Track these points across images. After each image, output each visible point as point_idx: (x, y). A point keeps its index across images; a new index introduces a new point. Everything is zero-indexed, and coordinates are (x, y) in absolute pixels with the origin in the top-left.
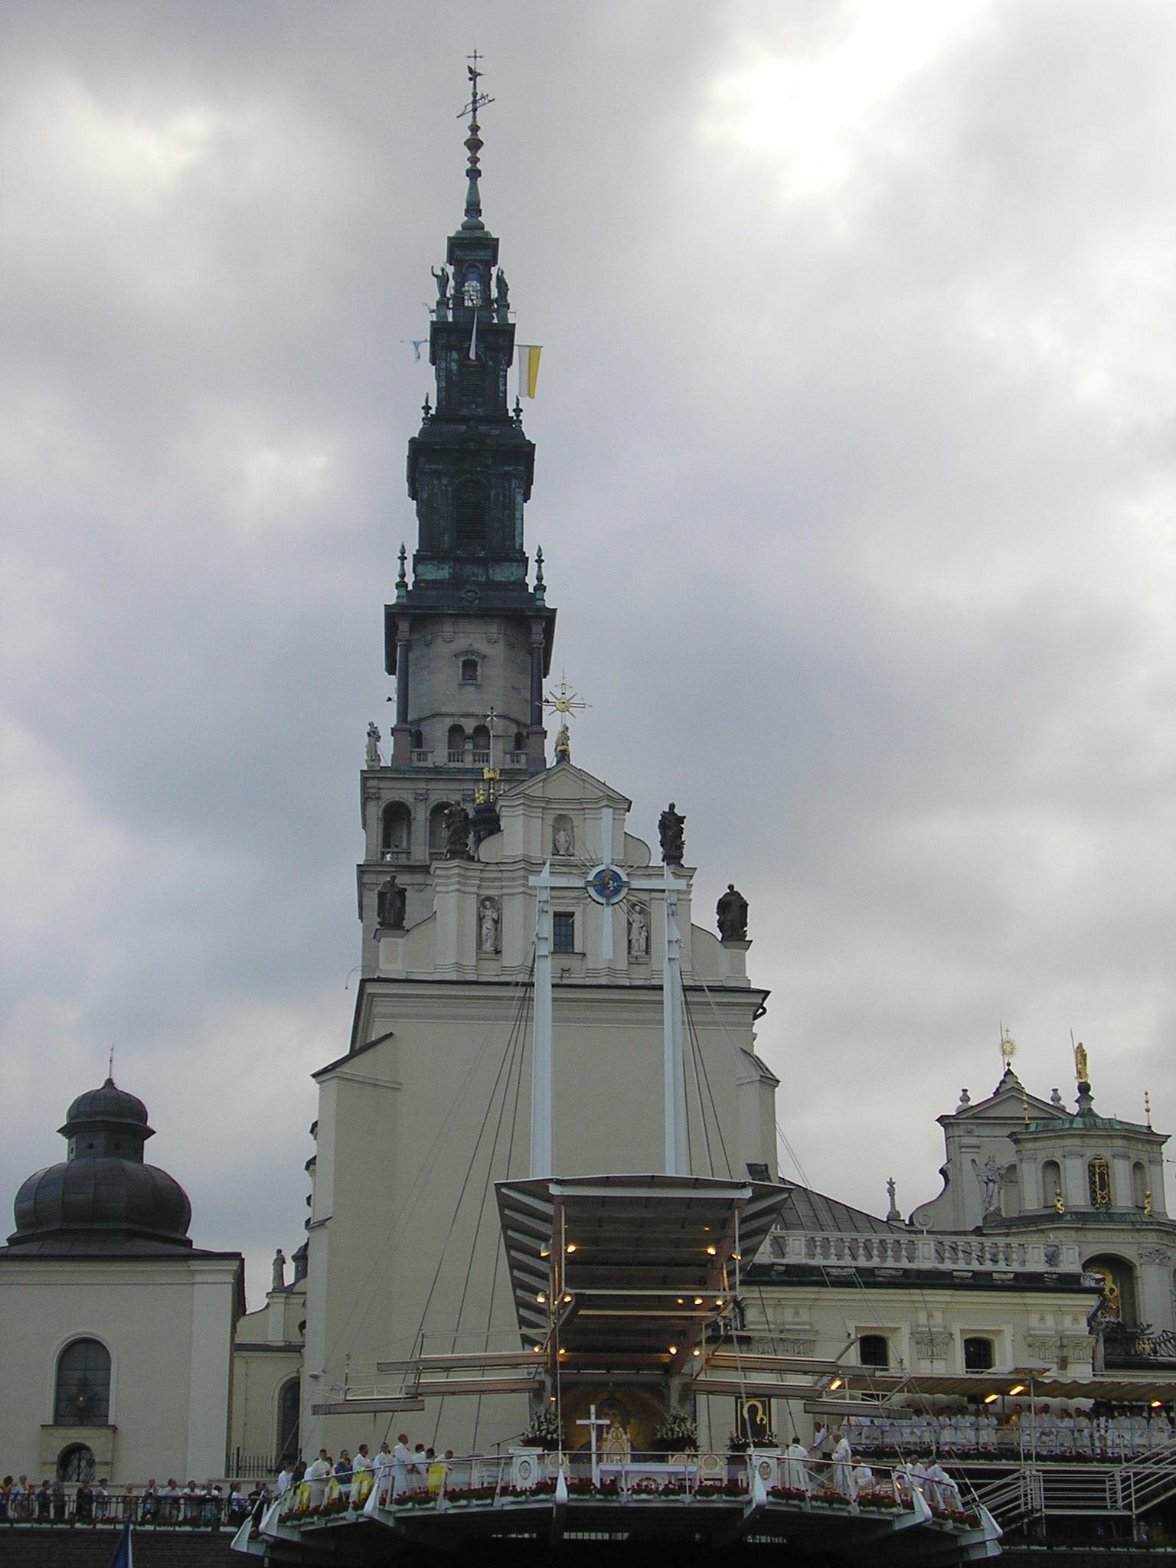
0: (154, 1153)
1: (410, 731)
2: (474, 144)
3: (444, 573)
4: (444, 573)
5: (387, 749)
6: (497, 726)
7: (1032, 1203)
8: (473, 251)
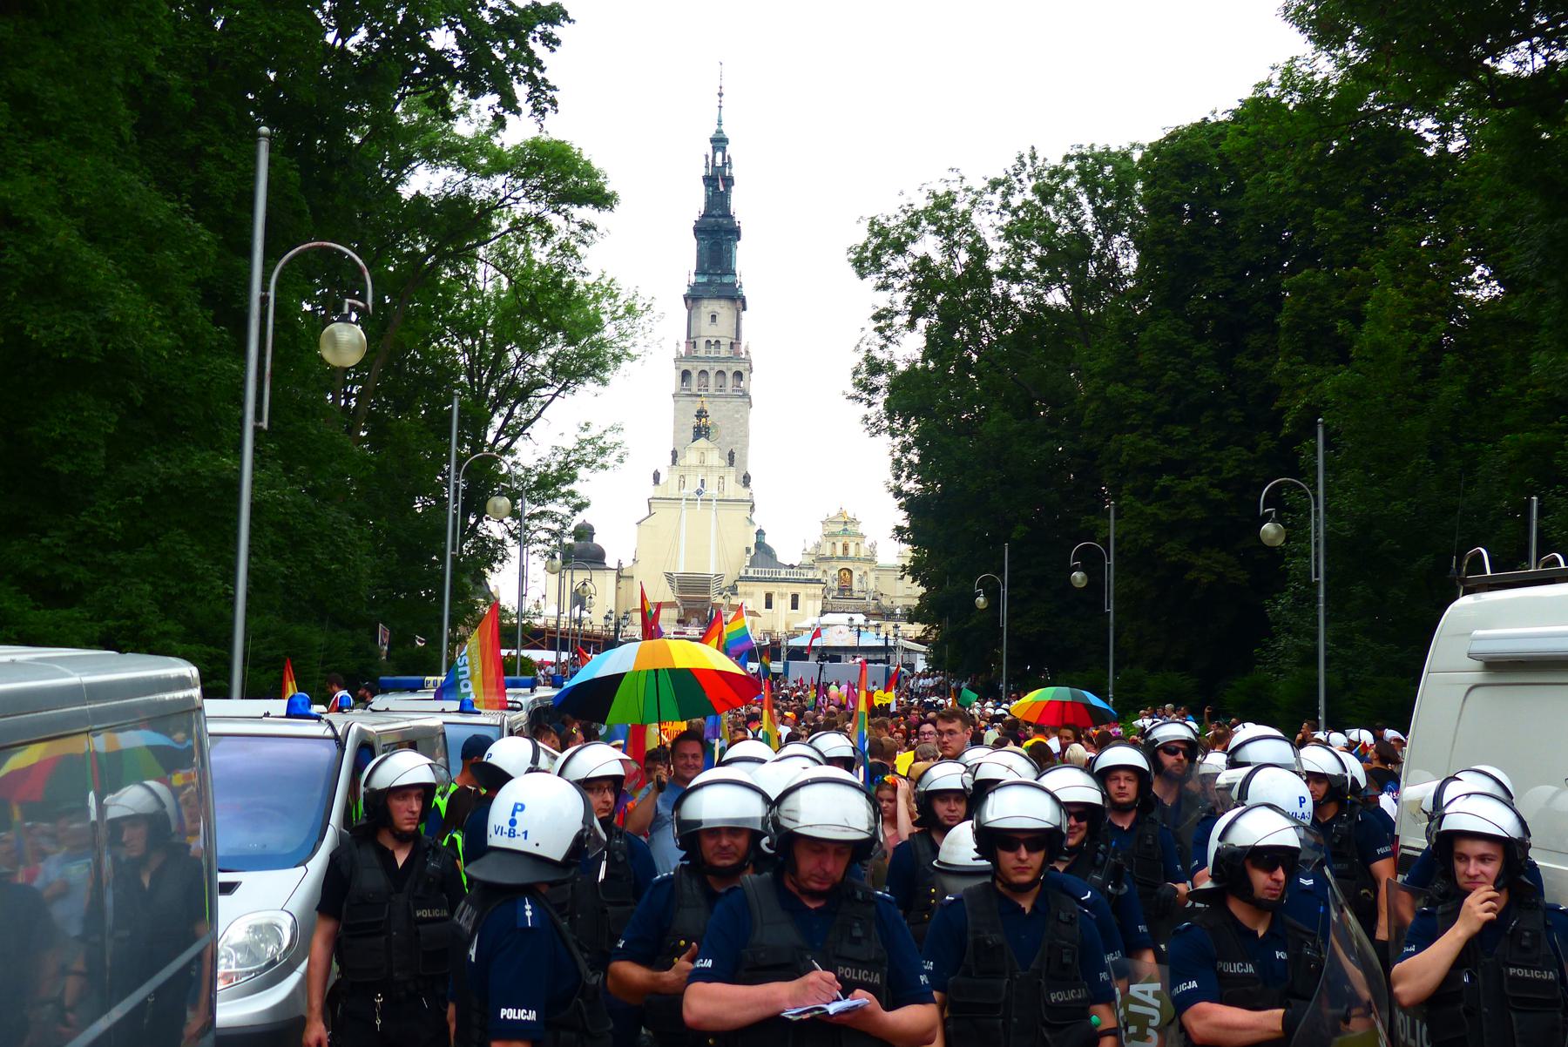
0: (596, 540)
1: (692, 342)
2: (721, 95)
3: (704, 279)
4: (704, 279)
5: (683, 349)
6: (723, 341)
7: (828, 554)
8: (719, 142)
